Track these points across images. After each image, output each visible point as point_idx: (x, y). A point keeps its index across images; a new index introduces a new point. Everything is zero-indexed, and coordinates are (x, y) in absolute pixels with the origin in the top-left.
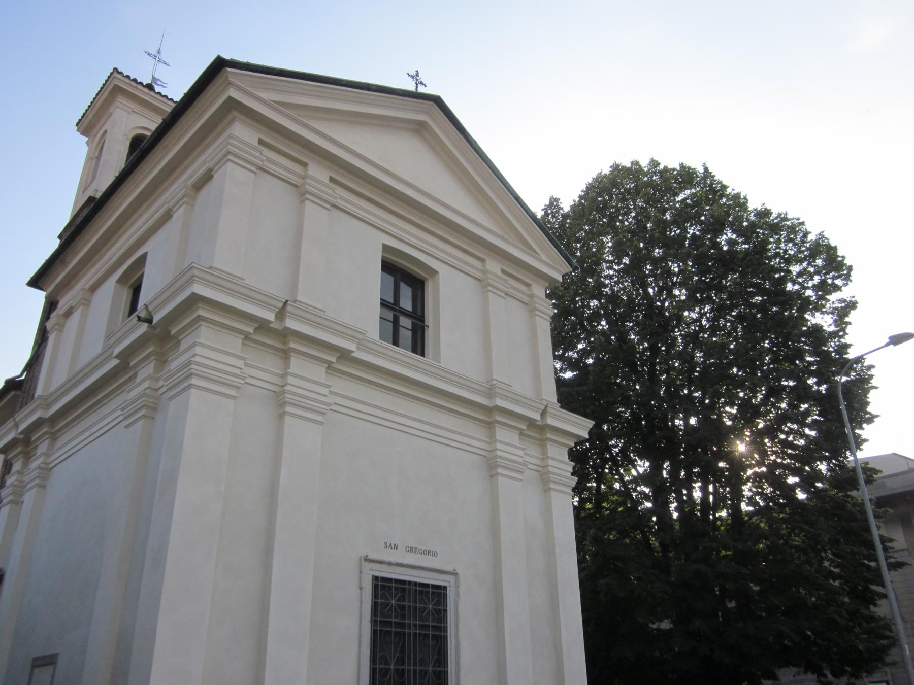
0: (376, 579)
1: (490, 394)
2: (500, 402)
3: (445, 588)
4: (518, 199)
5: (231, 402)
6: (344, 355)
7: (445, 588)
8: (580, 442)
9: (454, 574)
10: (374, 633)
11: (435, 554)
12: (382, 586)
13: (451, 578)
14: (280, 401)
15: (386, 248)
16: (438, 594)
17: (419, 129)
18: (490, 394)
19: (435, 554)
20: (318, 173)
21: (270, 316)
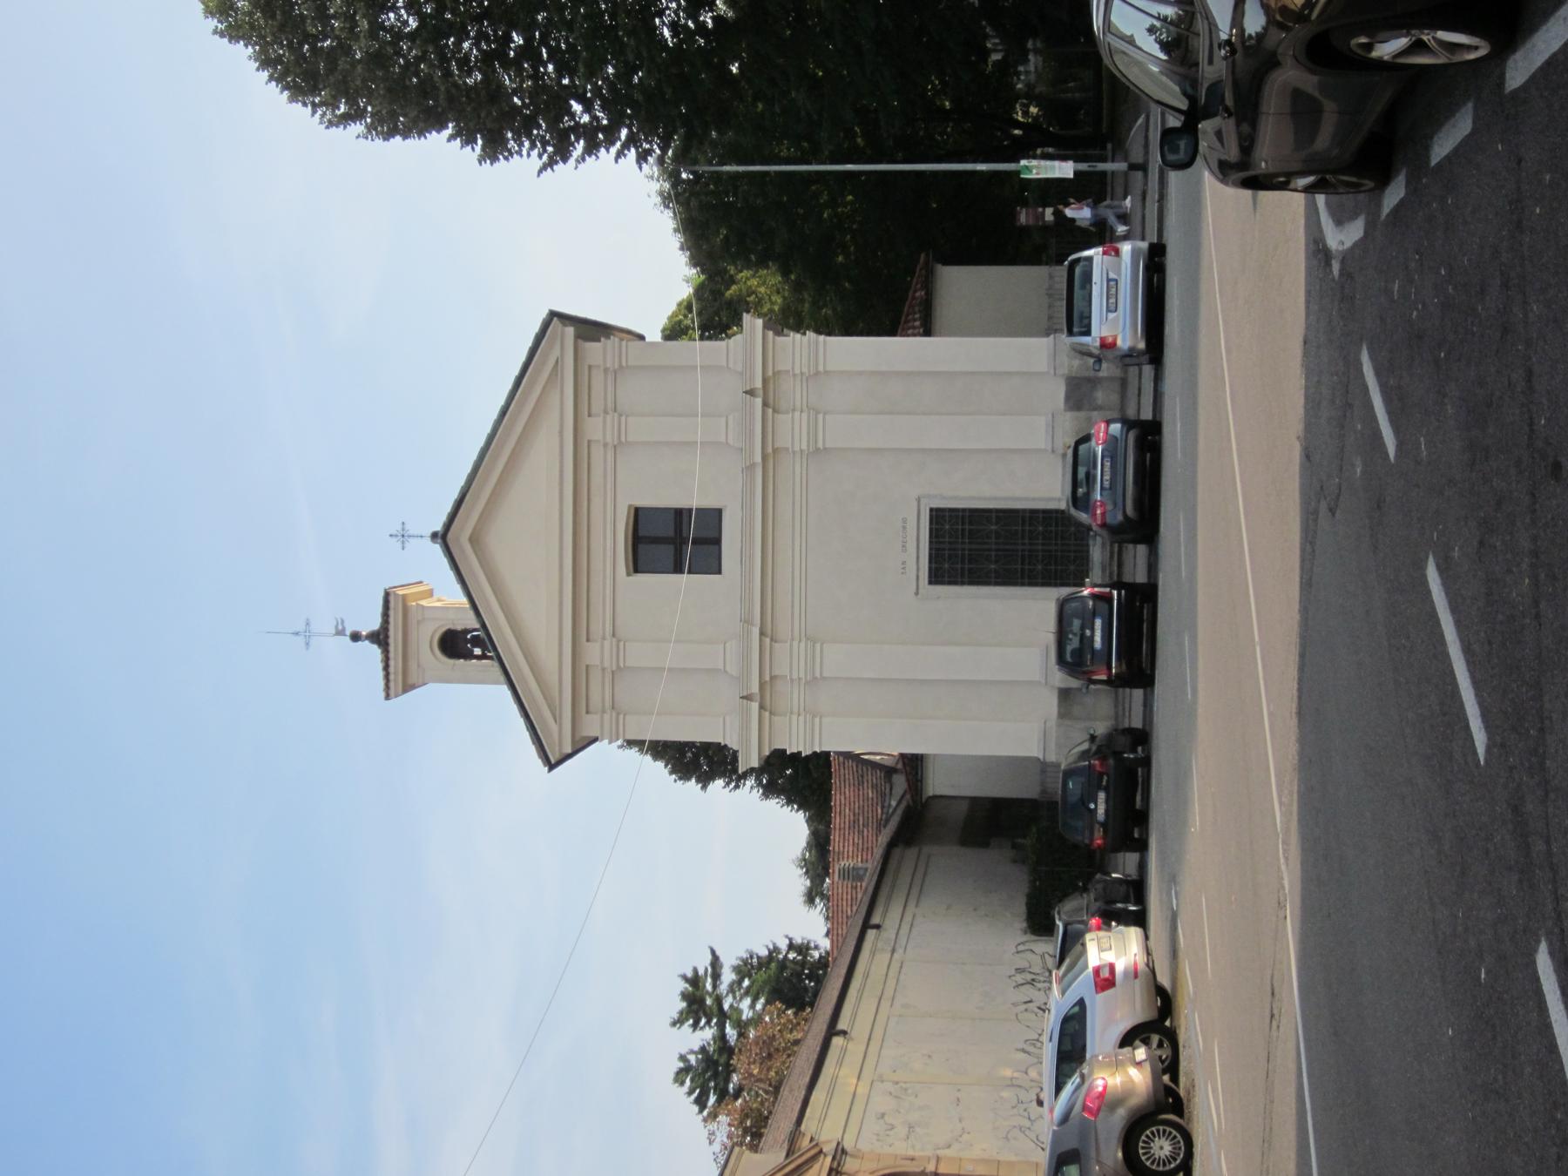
0: (930, 583)
1: (752, 466)
2: (758, 459)
3: (931, 510)
4: (504, 412)
5: (825, 720)
6: (762, 634)
7: (931, 510)
8: (766, 327)
9: (919, 500)
10: (971, 583)
11: (904, 521)
12: (936, 577)
13: (923, 502)
14: (813, 681)
15: (628, 574)
16: (939, 517)
17: (475, 540)
18: (752, 466)
19: (904, 521)
20: (593, 653)
21: (755, 706)
